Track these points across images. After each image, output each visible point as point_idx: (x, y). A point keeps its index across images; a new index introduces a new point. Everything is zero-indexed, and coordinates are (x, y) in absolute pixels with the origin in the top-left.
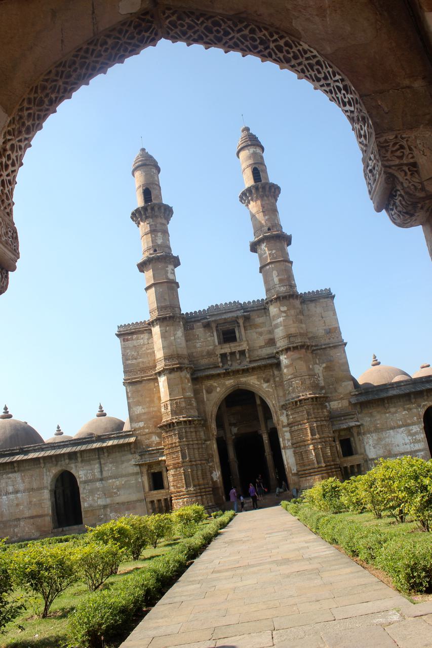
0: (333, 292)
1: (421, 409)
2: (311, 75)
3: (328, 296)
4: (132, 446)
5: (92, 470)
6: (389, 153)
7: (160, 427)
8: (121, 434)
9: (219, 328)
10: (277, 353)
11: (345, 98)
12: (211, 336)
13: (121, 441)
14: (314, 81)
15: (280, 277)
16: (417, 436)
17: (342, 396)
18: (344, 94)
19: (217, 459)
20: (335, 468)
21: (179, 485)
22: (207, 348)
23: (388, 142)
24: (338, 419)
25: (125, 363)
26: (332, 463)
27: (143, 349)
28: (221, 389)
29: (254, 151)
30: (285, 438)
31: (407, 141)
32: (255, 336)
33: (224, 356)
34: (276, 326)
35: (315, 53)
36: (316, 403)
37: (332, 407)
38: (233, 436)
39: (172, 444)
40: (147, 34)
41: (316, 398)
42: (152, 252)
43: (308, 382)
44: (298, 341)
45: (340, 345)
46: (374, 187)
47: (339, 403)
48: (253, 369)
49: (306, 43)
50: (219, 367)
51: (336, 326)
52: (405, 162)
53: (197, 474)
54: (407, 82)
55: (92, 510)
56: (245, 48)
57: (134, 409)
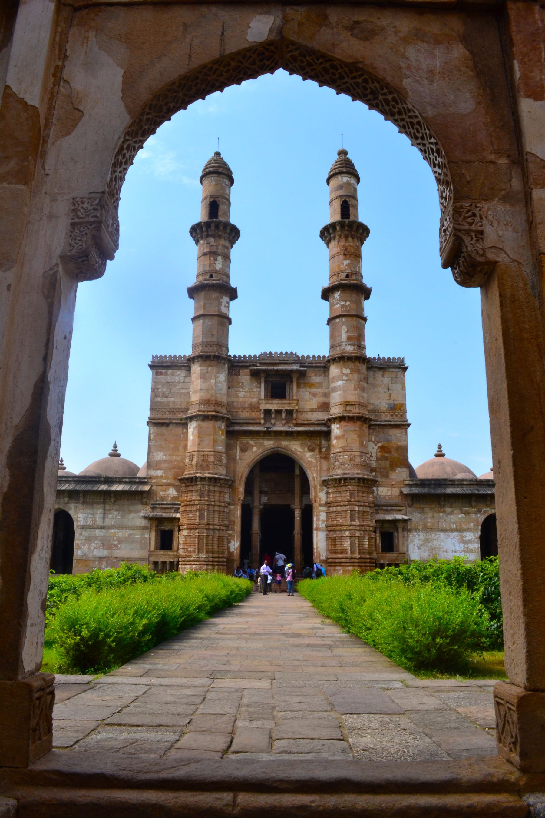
0: (407, 363)
1: (481, 515)
2: (410, 132)
3: (400, 366)
4: (144, 496)
5: (93, 514)
6: (462, 218)
7: (180, 480)
8: (134, 480)
10: (329, 420)
11: (436, 160)
12: (258, 387)
13: (134, 488)
14: (412, 138)
15: (350, 334)
16: (470, 545)
17: (393, 483)
18: (436, 157)
19: (238, 527)
20: (370, 562)
21: (189, 549)
22: (251, 400)
23: (463, 208)
24: (384, 508)
25: (154, 399)
26: (368, 556)
27: (177, 388)
28: (257, 450)
29: (347, 180)
30: (320, 519)
31: (480, 210)
32: (307, 396)
33: (267, 412)
34: (334, 390)
35: (417, 114)
36: (362, 485)
37: (380, 493)
38: (261, 505)
39: (191, 501)
40: (267, 63)
41: (364, 479)
42: (207, 277)
43: (358, 460)
44: (356, 411)
45: (403, 425)
46: (444, 245)
47: (388, 490)
48: (299, 433)
49: (410, 103)
50: (260, 423)
51: (402, 402)
52: (474, 229)
53: (212, 541)
54: (492, 157)
55: (85, 560)
56: (356, 94)
57: (155, 454)
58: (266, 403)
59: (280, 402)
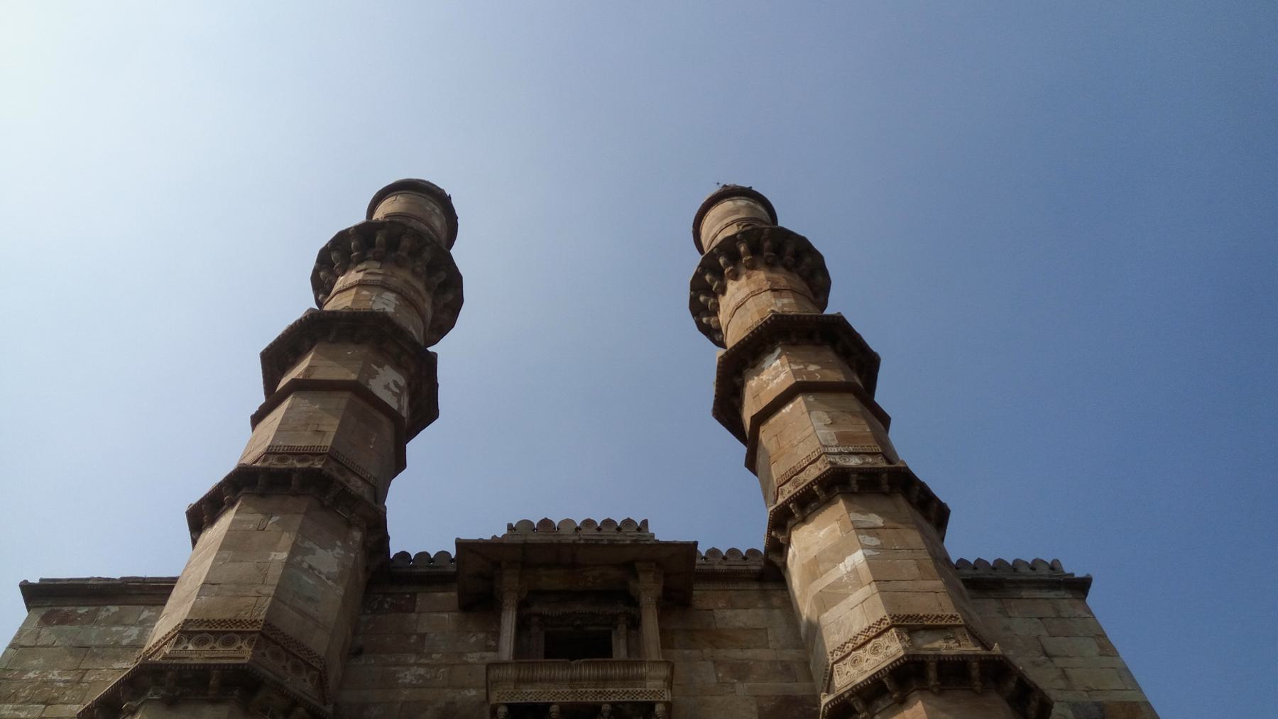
9: (536, 609)
22: (450, 694)
51: (1130, 696)
58: (519, 681)
59: (587, 672)
